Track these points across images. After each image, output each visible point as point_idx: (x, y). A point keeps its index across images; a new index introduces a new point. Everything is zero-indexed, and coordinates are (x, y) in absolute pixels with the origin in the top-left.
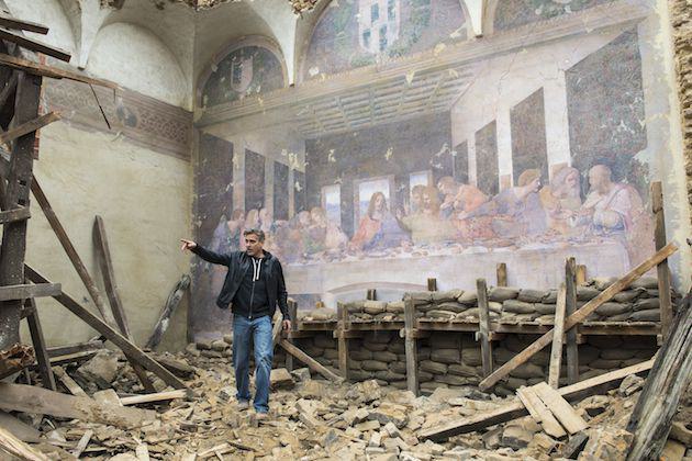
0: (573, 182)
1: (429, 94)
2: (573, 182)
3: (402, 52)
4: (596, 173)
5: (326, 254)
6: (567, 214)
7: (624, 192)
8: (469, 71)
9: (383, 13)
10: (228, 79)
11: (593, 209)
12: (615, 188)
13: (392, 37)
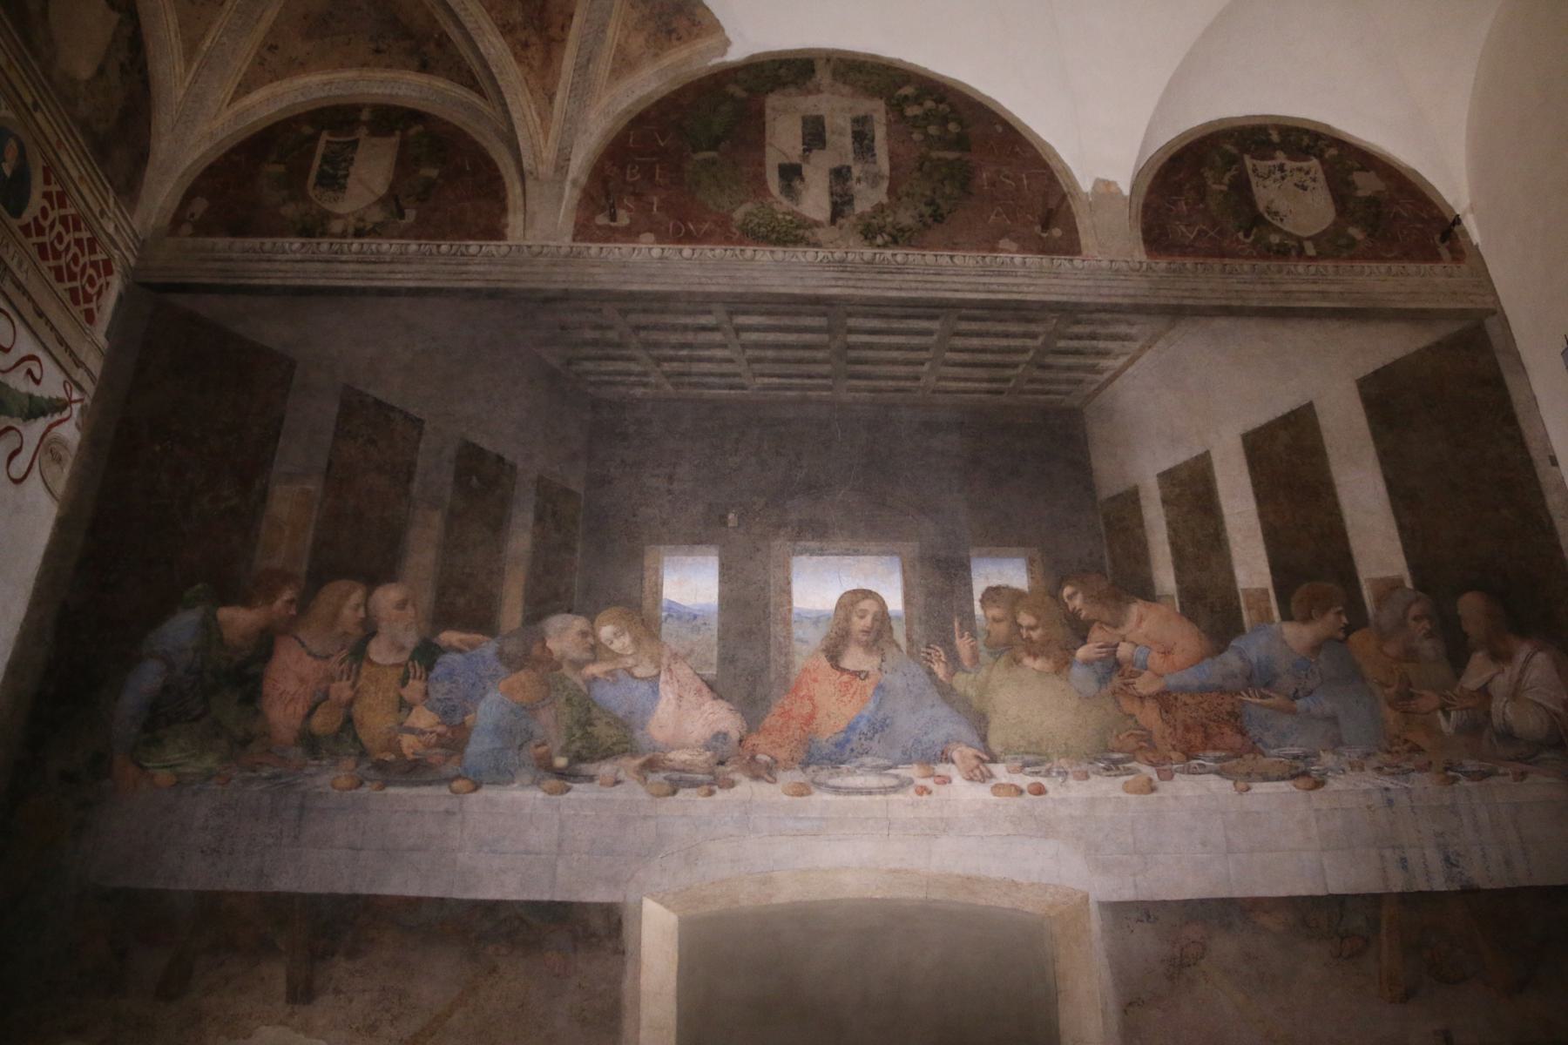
0: (1426, 624)
3: (899, 237)
4: (1471, 606)
5: (651, 765)
7: (1540, 658)
8: (1122, 329)
11: (1484, 692)
12: (1523, 651)
13: (868, 198)
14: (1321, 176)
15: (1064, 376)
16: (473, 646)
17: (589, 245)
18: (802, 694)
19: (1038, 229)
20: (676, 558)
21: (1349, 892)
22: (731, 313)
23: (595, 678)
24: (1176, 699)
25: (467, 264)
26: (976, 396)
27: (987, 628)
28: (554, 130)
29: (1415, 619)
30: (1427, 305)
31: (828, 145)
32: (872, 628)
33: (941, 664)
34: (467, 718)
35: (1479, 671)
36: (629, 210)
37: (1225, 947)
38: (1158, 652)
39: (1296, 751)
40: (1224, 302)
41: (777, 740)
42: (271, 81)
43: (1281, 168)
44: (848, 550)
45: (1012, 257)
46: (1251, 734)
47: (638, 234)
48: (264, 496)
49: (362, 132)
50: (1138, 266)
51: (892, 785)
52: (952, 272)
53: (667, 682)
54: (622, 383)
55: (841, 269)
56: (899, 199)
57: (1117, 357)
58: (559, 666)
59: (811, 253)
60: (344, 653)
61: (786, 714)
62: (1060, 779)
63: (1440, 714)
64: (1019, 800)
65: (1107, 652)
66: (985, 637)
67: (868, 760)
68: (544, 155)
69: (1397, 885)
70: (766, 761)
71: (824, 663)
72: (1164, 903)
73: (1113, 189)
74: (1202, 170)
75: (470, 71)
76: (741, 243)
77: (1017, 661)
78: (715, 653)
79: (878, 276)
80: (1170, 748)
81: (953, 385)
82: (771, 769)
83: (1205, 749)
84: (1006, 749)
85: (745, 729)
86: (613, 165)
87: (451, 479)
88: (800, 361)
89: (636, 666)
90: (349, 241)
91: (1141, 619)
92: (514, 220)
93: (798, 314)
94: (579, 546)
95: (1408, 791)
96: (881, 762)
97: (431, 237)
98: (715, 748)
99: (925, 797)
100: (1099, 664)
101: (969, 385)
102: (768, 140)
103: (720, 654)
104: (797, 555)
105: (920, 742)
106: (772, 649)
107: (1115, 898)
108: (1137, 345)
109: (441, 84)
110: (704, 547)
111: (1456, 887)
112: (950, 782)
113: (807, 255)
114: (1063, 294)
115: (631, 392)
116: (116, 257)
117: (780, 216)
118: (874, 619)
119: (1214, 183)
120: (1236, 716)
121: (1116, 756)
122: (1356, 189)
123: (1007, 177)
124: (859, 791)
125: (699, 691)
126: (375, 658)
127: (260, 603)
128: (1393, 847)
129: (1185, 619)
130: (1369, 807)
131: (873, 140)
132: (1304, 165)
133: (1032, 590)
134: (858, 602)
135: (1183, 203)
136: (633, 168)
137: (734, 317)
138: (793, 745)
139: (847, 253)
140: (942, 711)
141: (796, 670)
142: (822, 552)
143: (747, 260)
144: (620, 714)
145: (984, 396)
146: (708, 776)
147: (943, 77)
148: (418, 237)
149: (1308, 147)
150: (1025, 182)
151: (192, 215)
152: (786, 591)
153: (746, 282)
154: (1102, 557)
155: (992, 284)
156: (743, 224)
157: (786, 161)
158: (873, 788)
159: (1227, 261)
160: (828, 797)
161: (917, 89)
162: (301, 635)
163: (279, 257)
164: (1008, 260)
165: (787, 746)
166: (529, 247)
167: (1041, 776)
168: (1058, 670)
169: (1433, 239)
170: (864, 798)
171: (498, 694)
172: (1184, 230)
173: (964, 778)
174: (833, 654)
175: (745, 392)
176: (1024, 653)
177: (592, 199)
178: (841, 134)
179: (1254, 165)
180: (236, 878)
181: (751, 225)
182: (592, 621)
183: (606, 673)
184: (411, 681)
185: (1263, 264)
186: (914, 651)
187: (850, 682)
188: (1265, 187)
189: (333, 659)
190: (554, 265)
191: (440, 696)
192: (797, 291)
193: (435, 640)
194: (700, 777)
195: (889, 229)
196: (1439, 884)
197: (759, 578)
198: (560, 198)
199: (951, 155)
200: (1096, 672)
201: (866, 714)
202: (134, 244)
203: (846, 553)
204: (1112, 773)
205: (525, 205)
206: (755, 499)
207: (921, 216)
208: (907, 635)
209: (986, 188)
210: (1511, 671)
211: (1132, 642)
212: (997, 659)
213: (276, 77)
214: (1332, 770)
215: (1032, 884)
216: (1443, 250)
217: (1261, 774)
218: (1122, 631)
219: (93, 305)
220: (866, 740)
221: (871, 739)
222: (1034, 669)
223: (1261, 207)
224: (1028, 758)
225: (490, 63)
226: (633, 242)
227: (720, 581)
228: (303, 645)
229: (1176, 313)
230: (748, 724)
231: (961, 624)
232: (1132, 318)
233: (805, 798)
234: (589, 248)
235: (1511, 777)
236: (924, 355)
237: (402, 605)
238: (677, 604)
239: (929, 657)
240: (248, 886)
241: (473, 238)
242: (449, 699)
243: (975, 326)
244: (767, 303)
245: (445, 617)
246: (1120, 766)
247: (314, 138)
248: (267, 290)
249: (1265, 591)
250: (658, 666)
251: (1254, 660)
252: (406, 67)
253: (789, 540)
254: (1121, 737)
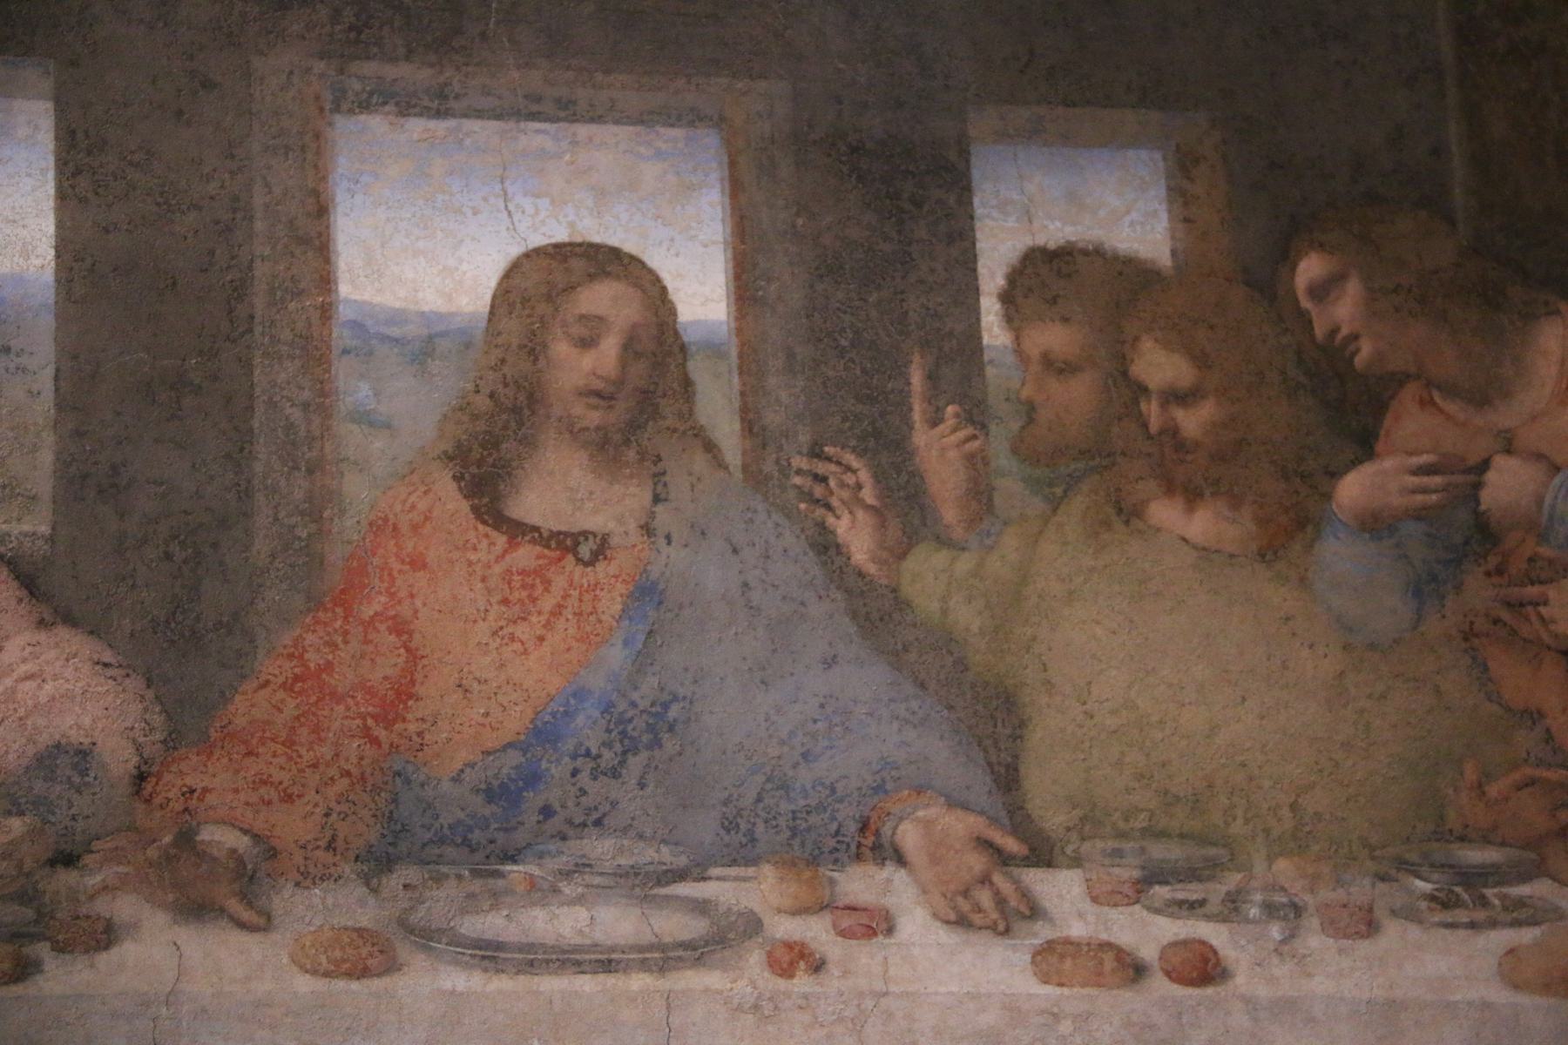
18: (368, 612)
27: (1025, 393)
32: (620, 382)
33: (860, 514)
41: (277, 775)
44: (539, 99)
51: (686, 936)
62: (1275, 931)
64: (1131, 1001)
65: (1445, 489)
66: (1015, 426)
67: (600, 847)
70: (234, 851)
77: (1130, 513)
78: (47, 457)
82: (252, 878)
84: (1083, 819)
85: (158, 736)
96: (648, 855)
99: (802, 983)
100: (1411, 528)
103: (63, 463)
104: (351, 111)
105: (785, 787)
106: (262, 449)
112: (890, 931)
118: (630, 348)
121: (1475, 856)
124: (567, 959)
134: (571, 288)
138: (332, 792)
141: (349, 527)
142: (440, 104)
146: (17, 908)
158: (613, 949)
160: (458, 980)
165: (311, 796)
167: (1209, 918)
170: (587, 984)
173: (935, 916)
176: (1151, 486)
186: (769, 467)
187: (537, 572)
197: (212, 188)
201: (596, 682)
203: (530, 110)
204: (1462, 916)
208: (744, 410)
211: (1540, 457)
212: (1055, 505)
218: (1505, 416)
221: (615, 773)
222: (1184, 539)
224: (1160, 851)
227: (62, 196)
230: (169, 718)
231: (932, 378)
233: (377, 984)
239: (818, 491)
253: (322, 56)
254: (1493, 790)
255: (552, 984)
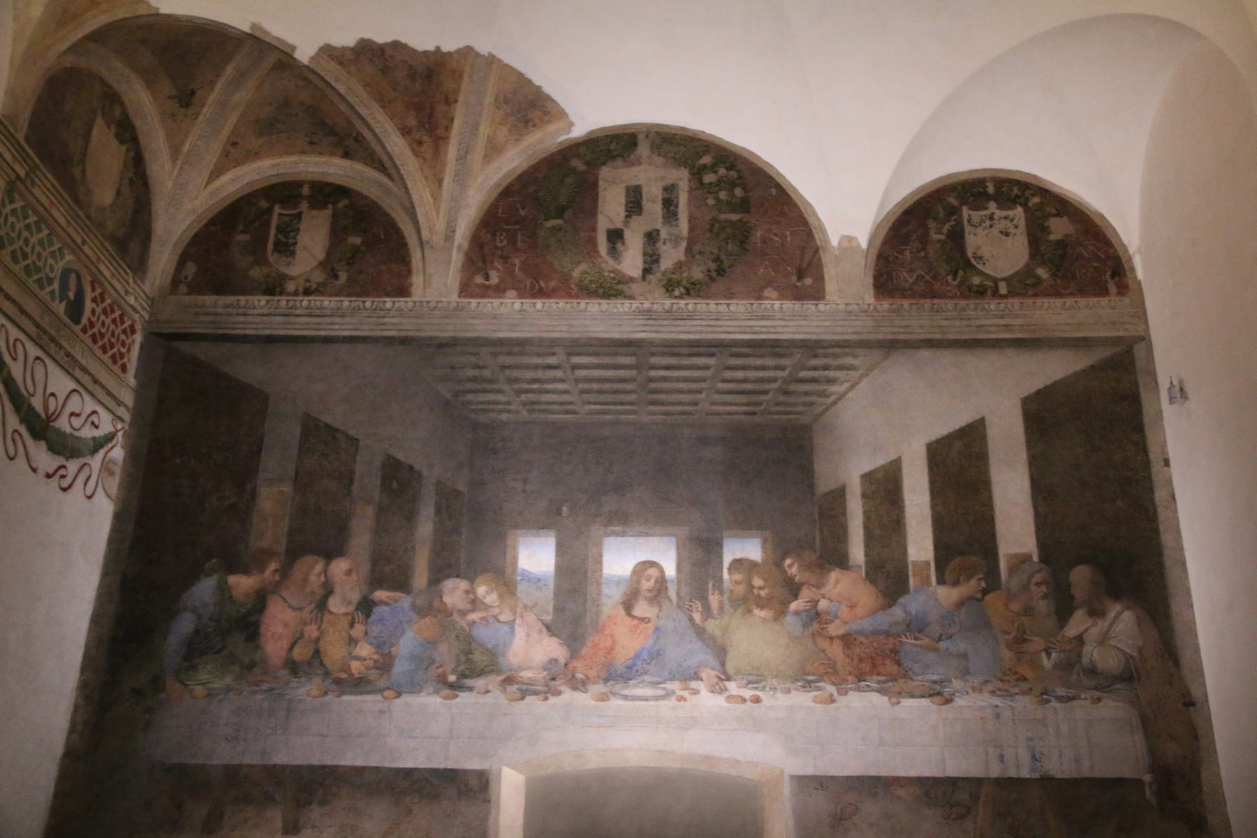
0: (1044, 588)
1: (767, 386)
2: (1044, 588)
3: (692, 290)
4: (1080, 577)
5: (509, 681)
6: (1037, 644)
7: (1128, 616)
8: (848, 361)
9: (653, 207)
10: (259, 241)
11: (1080, 640)
12: (1114, 608)
13: (671, 256)
14: (1022, 223)
15: (802, 399)
16: (396, 601)
17: (470, 300)
19: (794, 278)
20: (527, 539)
21: (961, 776)
22: (569, 354)
23: (474, 622)
24: (855, 639)
25: (383, 317)
26: (736, 417)
27: (731, 588)
28: (444, 206)
29: (1038, 584)
30: (1090, 334)
31: (644, 212)
32: (654, 588)
34: (393, 649)
35: (1078, 623)
36: (498, 270)
37: (871, 808)
38: (847, 606)
39: (935, 677)
40: (929, 336)
42: (235, 167)
43: (991, 218)
45: (774, 304)
46: (905, 665)
47: (505, 290)
48: (254, 495)
49: (304, 206)
50: (866, 307)
52: (728, 318)
53: (520, 624)
54: (492, 410)
55: (648, 317)
56: (693, 257)
57: (842, 383)
58: (451, 615)
59: (627, 303)
60: (312, 606)
61: (595, 646)
62: (771, 693)
63: (1043, 655)
64: (743, 706)
67: (646, 678)
68: (437, 228)
69: (995, 772)
71: (622, 612)
72: (833, 778)
73: (854, 244)
74: (927, 222)
75: (380, 161)
76: (577, 297)
77: (749, 611)
78: (551, 605)
79: (675, 323)
80: (847, 672)
81: (721, 409)
83: (872, 674)
86: (488, 232)
87: (379, 483)
88: (615, 392)
89: (500, 614)
90: (300, 298)
91: (837, 582)
92: (417, 280)
93: (615, 354)
94: (464, 530)
95: (1012, 708)
97: (358, 296)
98: (550, 669)
99: (682, 703)
101: (734, 408)
102: (600, 209)
103: (555, 605)
105: (680, 666)
107: (801, 773)
108: (854, 375)
109: (359, 167)
110: (546, 531)
111: (1037, 775)
113: (623, 306)
114: (807, 333)
115: (500, 417)
116: (137, 319)
117: (606, 274)
118: (656, 582)
119: (935, 233)
120: (895, 651)
122: (1049, 233)
123: (775, 235)
125: (540, 631)
126: (332, 609)
127: (255, 572)
128: (996, 746)
129: (868, 583)
130: (981, 718)
131: (677, 207)
132: (1010, 213)
133: (765, 561)
134: (646, 570)
135: (908, 251)
136: (501, 235)
137: (571, 358)
139: (653, 304)
140: (697, 645)
141: (603, 617)
142: (623, 534)
143: (581, 311)
144: (490, 646)
145: (742, 417)
147: (734, 145)
148: (349, 295)
149: (1017, 196)
150: (789, 239)
151: (186, 277)
152: (599, 562)
153: (579, 329)
154: (814, 538)
155: (755, 326)
156: (580, 281)
157: (612, 227)
159: (936, 301)
160: (620, 702)
161: (713, 158)
162: (283, 594)
163: (251, 312)
164: (769, 306)
166: (428, 302)
168: (776, 619)
169: (1105, 275)
170: (643, 703)
171: (412, 633)
172: (906, 276)
174: (628, 605)
175: (577, 416)
176: (754, 606)
177: (472, 261)
178: (654, 202)
179: (969, 215)
180: (250, 757)
181: (586, 282)
182: (472, 583)
183: (483, 619)
184: (356, 625)
185: (963, 303)
186: (681, 604)
188: (975, 235)
189: (306, 610)
190: (446, 317)
191: (375, 634)
192: (616, 336)
193: (371, 597)
194: (540, 688)
195: (684, 283)
196: (1025, 773)
198: (449, 262)
199: (734, 217)
200: (802, 620)
202: (147, 303)
203: (640, 535)
204: (806, 689)
205: (424, 269)
206: (581, 496)
207: (709, 271)
209: (759, 245)
210: (1102, 625)
211: (829, 599)
212: (736, 610)
213: (238, 163)
214: (959, 692)
215: (748, 762)
216: (1112, 288)
217: (908, 693)
218: (823, 591)
219: (125, 360)
220: (647, 664)
223: (970, 254)
225: (395, 158)
226: (501, 298)
227: (557, 555)
228: (284, 600)
229: (891, 346)
231: (713, 585)
232: (857, 351)
234: (470, 303)
235: (1089, 701)
236: (703, 385)
237: (349, 573)
238: (527, 571)
240: (255, 760)
241: (388, 295)
242: (381, 637)
243: (740, 361)
244: (595, 346)
245: (377, 581)
246: (812, 685)
247: (269, 211)
248: (244, 339)
249: (928, 563)
250: (515, 614)
251: (914, 613)
252: (332, 154)
254: (816, 664)
255: (637, 703)
